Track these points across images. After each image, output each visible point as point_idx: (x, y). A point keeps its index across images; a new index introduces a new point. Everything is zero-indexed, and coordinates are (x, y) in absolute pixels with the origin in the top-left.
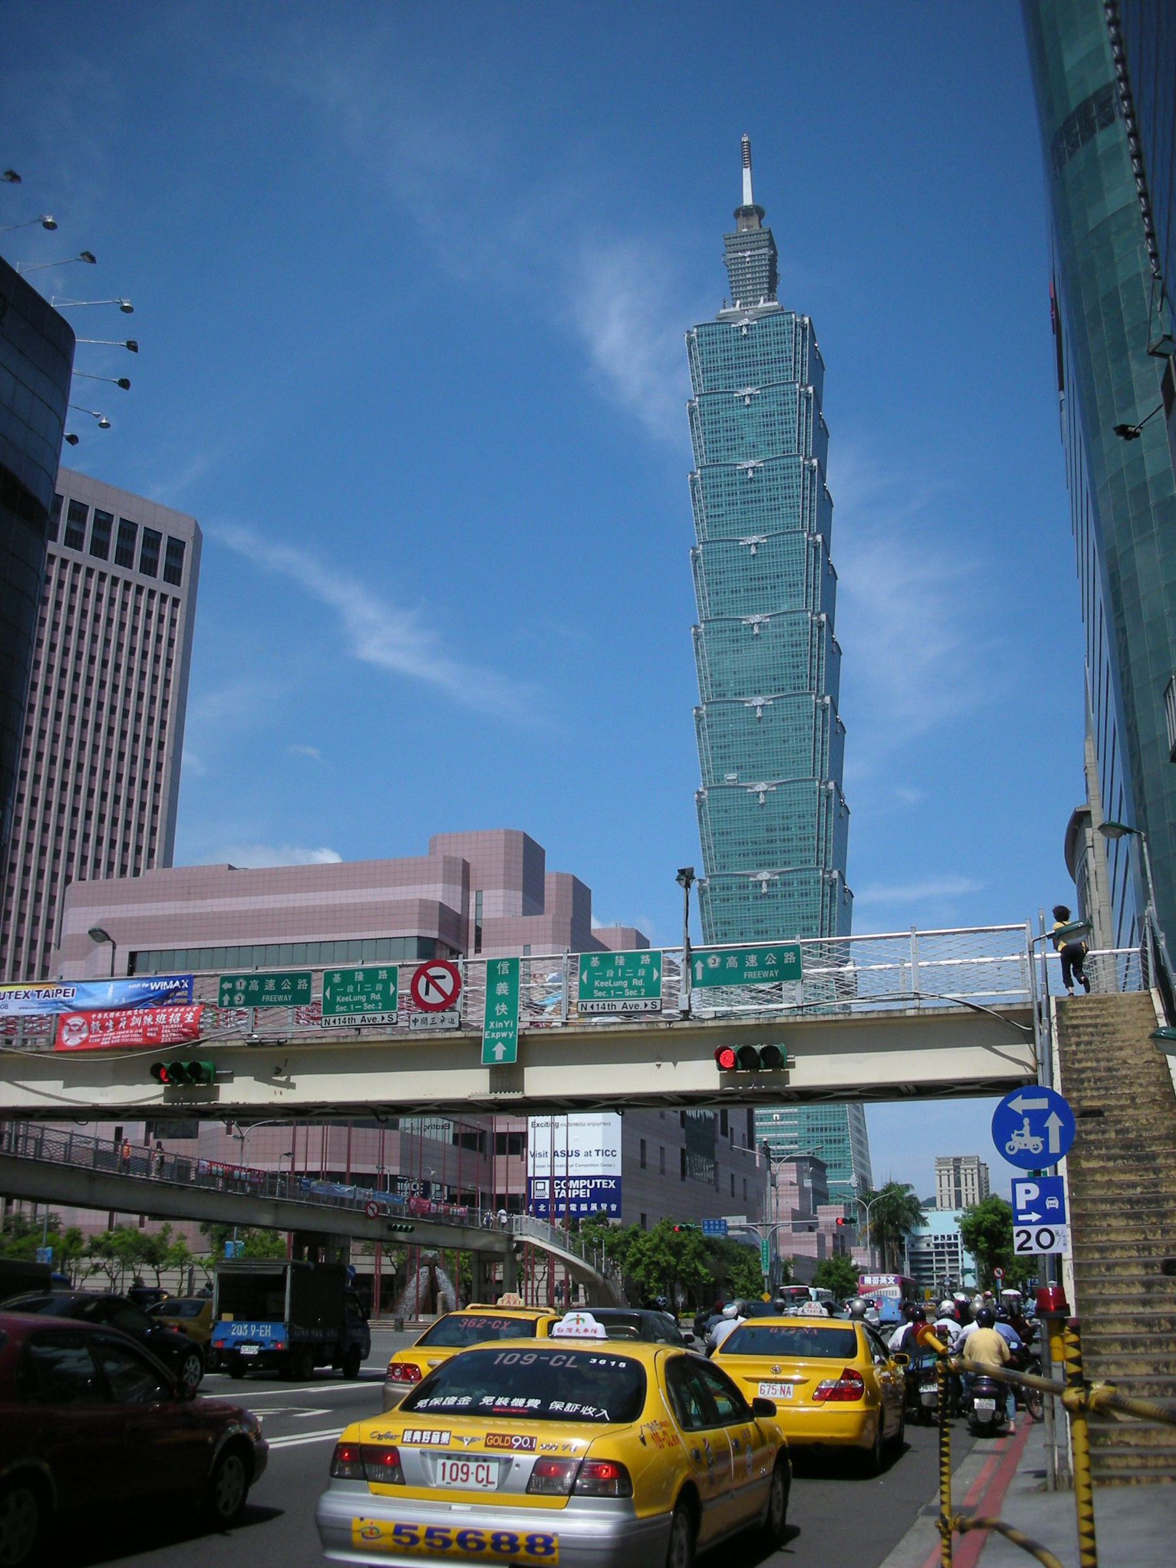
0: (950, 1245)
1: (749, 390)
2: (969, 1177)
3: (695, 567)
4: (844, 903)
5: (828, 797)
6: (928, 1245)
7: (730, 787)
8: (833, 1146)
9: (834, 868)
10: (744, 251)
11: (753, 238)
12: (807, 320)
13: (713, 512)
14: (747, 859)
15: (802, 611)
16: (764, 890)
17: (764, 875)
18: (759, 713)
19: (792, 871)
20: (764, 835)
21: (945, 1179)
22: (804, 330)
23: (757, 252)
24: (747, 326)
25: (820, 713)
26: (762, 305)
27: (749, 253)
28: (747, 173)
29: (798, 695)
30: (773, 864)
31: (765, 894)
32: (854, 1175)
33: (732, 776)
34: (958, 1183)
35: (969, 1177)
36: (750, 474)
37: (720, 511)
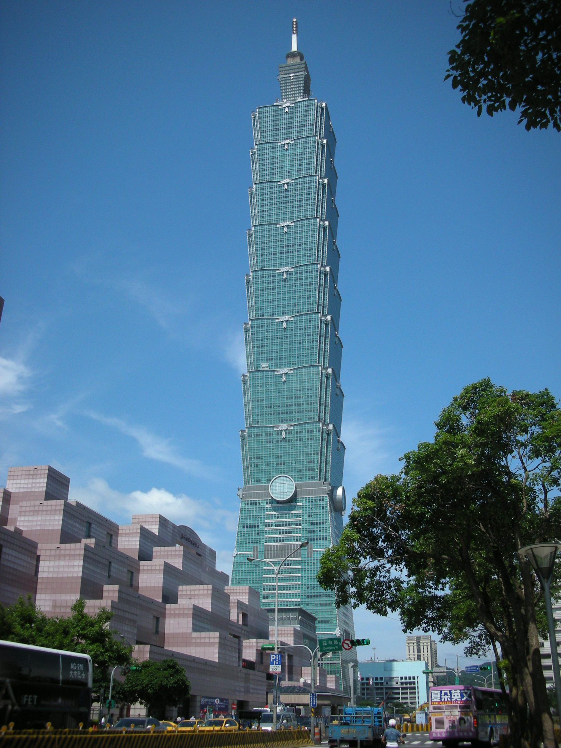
0: (410, 683)
1: (288, 141)
2: (425, 647)
3: (249, 242)
4: (338, 449)
5: (327, 378)
6: (397, 683)
7: (263, 371)
8: (324, 608)
9: (330, 423)
10: (290, 74)
11: (296, 67)
12: (324, 105)
13: (261, 209)
14: (273, 417)
15: (314, 264)
16: (284, 435)
17: (284, 426)
18: (285, 325)
19: (302, 424)
20: (284, 401)
21: (411, 648)
22: (322, 109)
23: (297, 74)
24: (288, 107)
25: (324, 326)
26: (299, 99)
27: (293, 75)
28: (294, 38)
29: (310, 314)
30: (291, 420)
31: (284, 439)
32: (338, 629)
33: (265, 365)
34: (419, 651)
35: (425, 647)
36: (286, 187)
37: (265, 208)
